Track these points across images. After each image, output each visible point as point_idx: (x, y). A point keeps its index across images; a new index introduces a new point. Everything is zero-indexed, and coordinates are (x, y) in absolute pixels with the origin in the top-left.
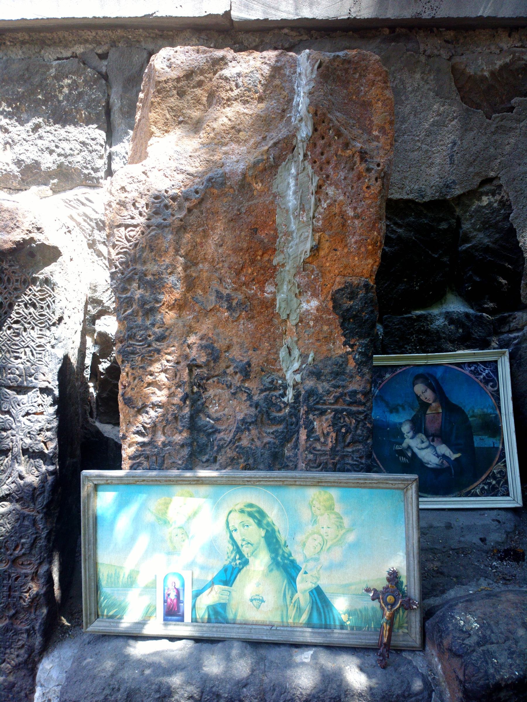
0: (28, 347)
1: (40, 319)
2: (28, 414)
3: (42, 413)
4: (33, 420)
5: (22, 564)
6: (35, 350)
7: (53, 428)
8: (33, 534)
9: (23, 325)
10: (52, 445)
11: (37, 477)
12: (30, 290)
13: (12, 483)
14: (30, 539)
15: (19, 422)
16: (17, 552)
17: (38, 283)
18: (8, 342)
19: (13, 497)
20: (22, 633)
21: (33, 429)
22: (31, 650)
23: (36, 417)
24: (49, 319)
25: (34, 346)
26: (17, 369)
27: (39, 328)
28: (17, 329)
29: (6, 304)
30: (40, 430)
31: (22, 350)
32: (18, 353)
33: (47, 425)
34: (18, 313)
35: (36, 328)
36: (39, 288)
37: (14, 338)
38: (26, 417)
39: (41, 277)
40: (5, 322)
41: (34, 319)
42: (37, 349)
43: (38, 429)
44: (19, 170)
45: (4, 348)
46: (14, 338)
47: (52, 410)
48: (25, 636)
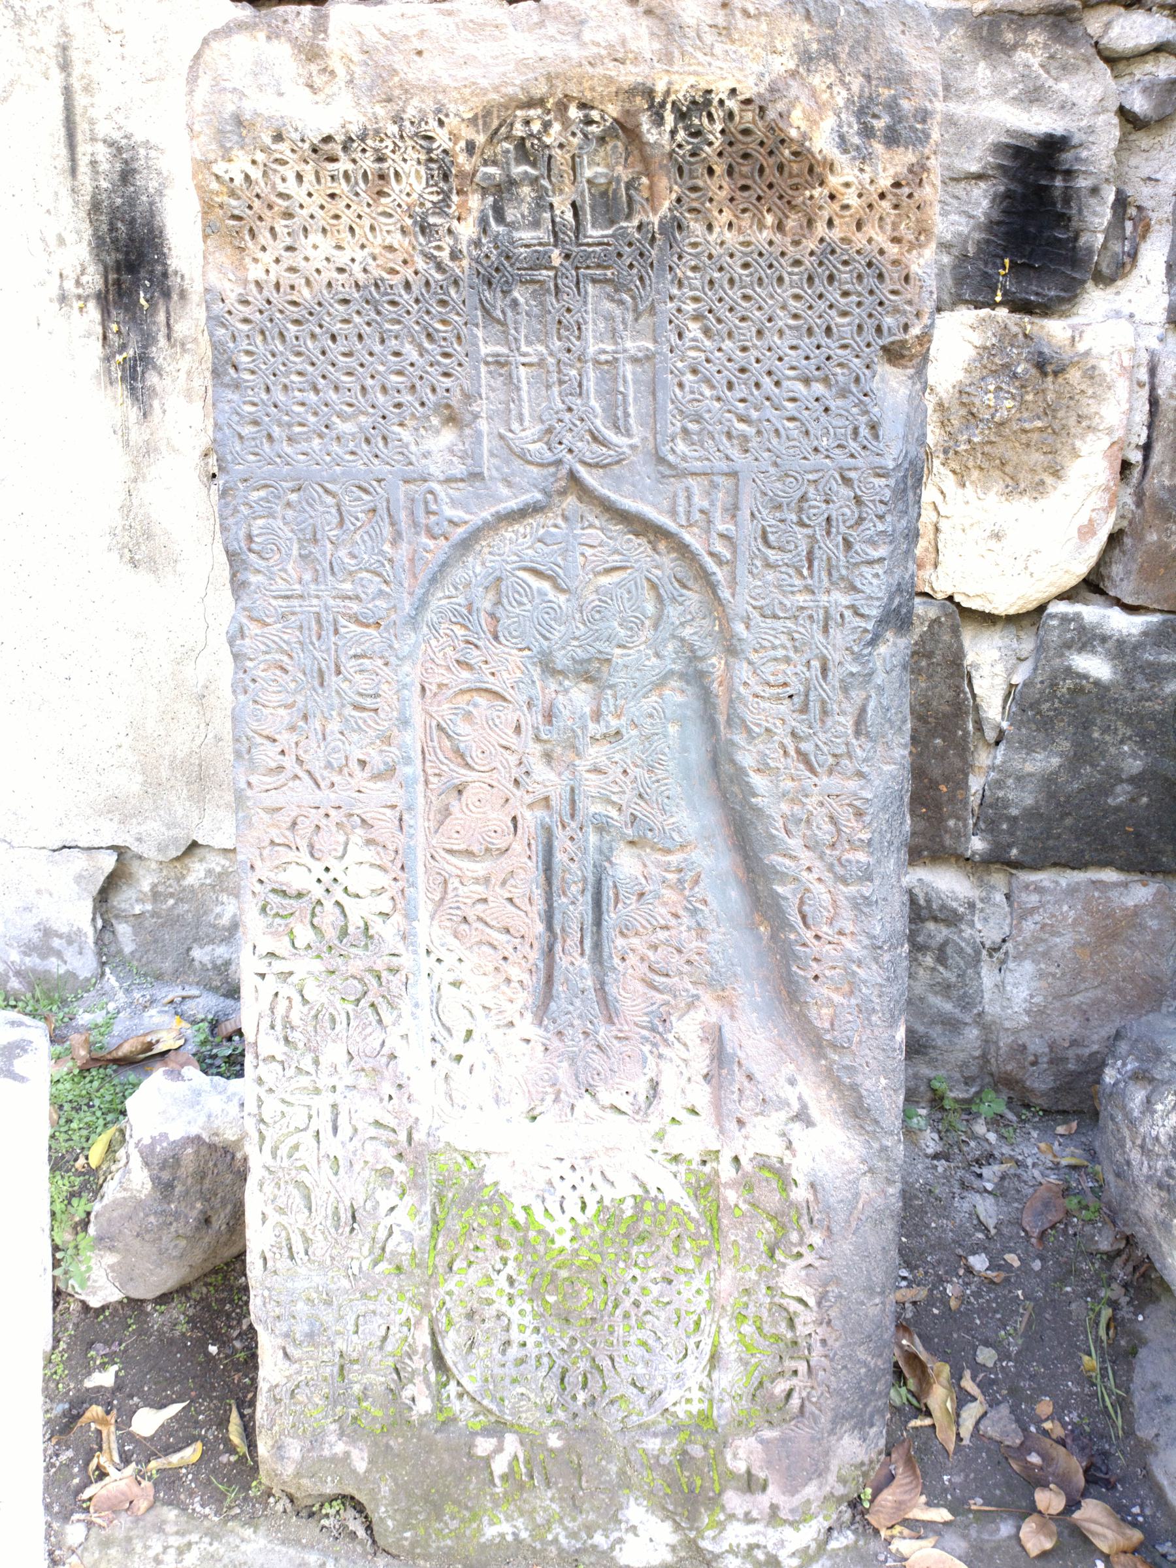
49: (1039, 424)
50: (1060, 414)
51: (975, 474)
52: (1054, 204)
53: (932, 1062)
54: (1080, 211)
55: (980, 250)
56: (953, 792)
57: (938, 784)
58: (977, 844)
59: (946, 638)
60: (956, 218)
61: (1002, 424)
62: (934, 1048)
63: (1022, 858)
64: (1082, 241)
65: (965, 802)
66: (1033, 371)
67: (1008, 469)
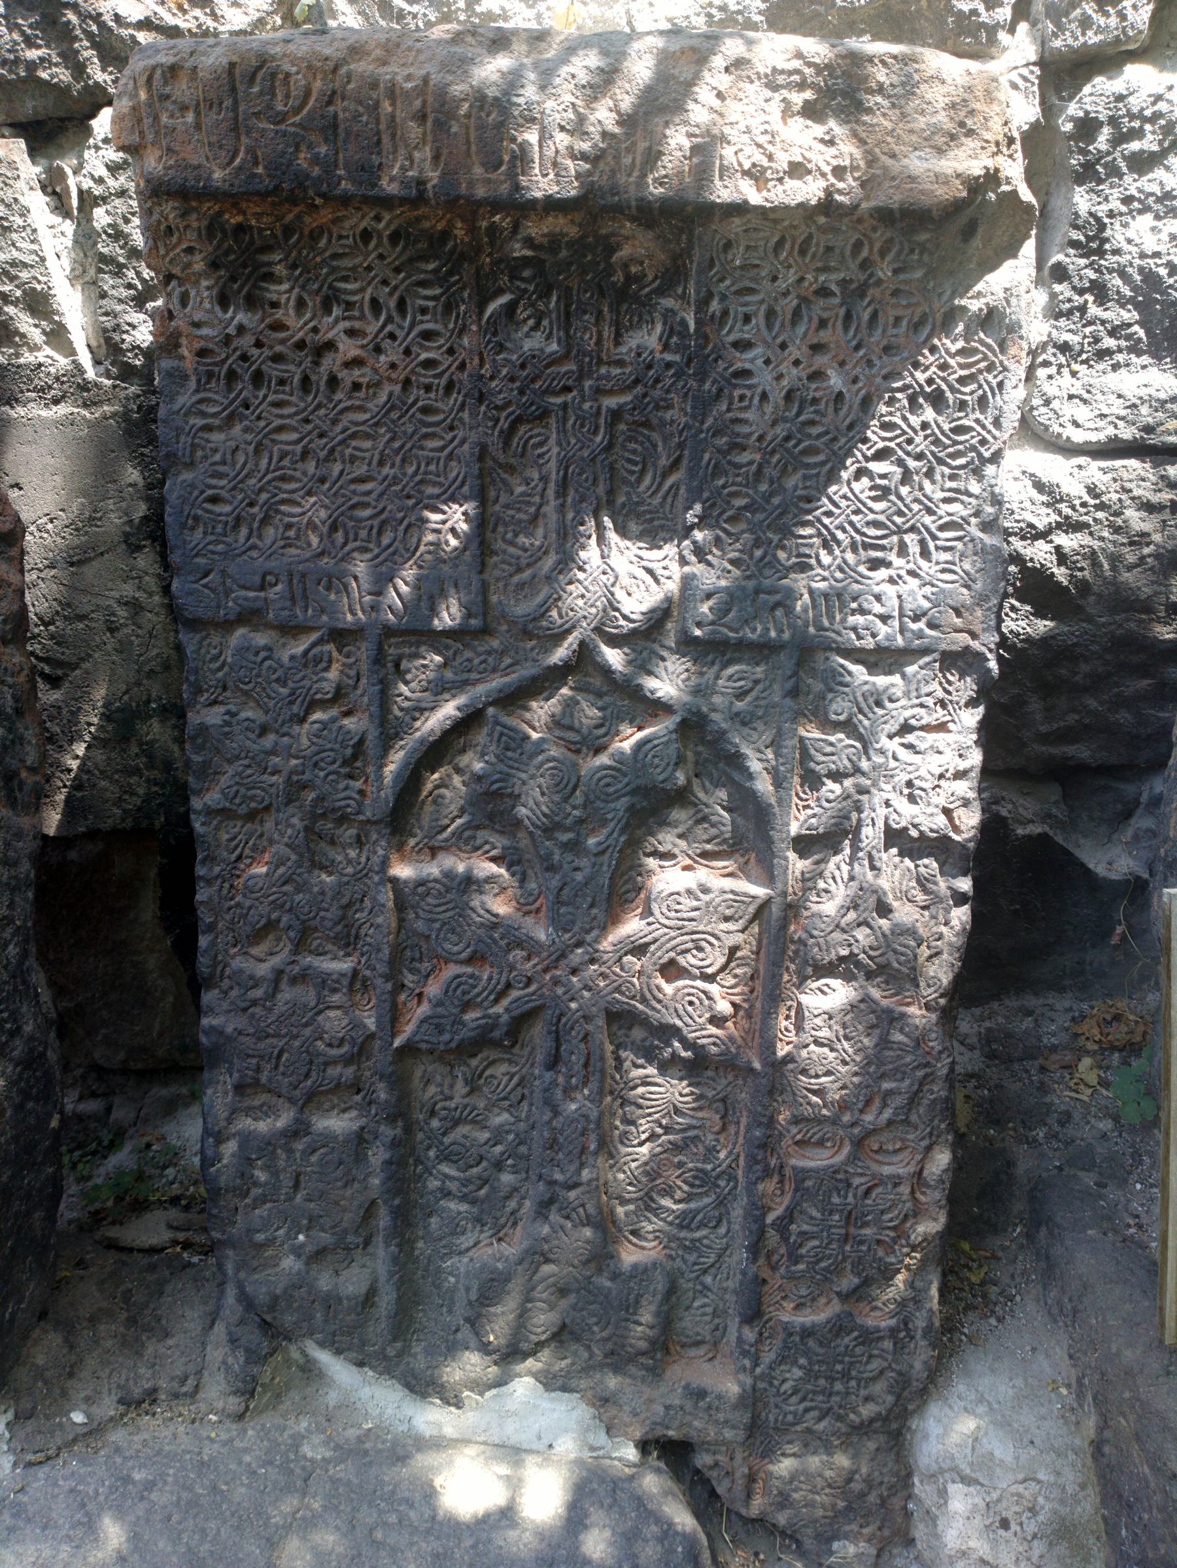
0: (913, 529)
1: (955, 443)
2: (906, 729)
3: (942, 727)
4: (922, 746)
5: (880, 1150)
6: (934, 538)
7: (971, 769)
8: (917, 1067)
9: (900, 463)
10: (970, 819)
11: (924, 908)
12: (933, 349)
13: (859, 925)
14: (907, 1082)
15: (882, 752)
16: (868, 1118)
17: (960, 327)
18: (854, 518)
19: (858, 964)
20: (881, 1338)
21: (923, 772)
22: (902, 1383)
23: (932, 738)
24: (983, 442)
25: (933, 528)
26: (878, 598)
27: (947, 471)
28: (883, 476)
29: (853, 399)
30: (941, 776)
31: (895, 539)
32: (883, 548)
33: (958, 760)
34: (886, 426)
35: (940, 469)
36: (960, 344)
37: (870, 503)
38: (897, 740)
39: (974, 305)
40: (849, 453)
41: (937, 442)
42: (940, 534)
43: (937, 771)
44: (763, 6)
45: (840, 535)
46: (870, 503)
47: (972, 718)
48: (888, 1344)
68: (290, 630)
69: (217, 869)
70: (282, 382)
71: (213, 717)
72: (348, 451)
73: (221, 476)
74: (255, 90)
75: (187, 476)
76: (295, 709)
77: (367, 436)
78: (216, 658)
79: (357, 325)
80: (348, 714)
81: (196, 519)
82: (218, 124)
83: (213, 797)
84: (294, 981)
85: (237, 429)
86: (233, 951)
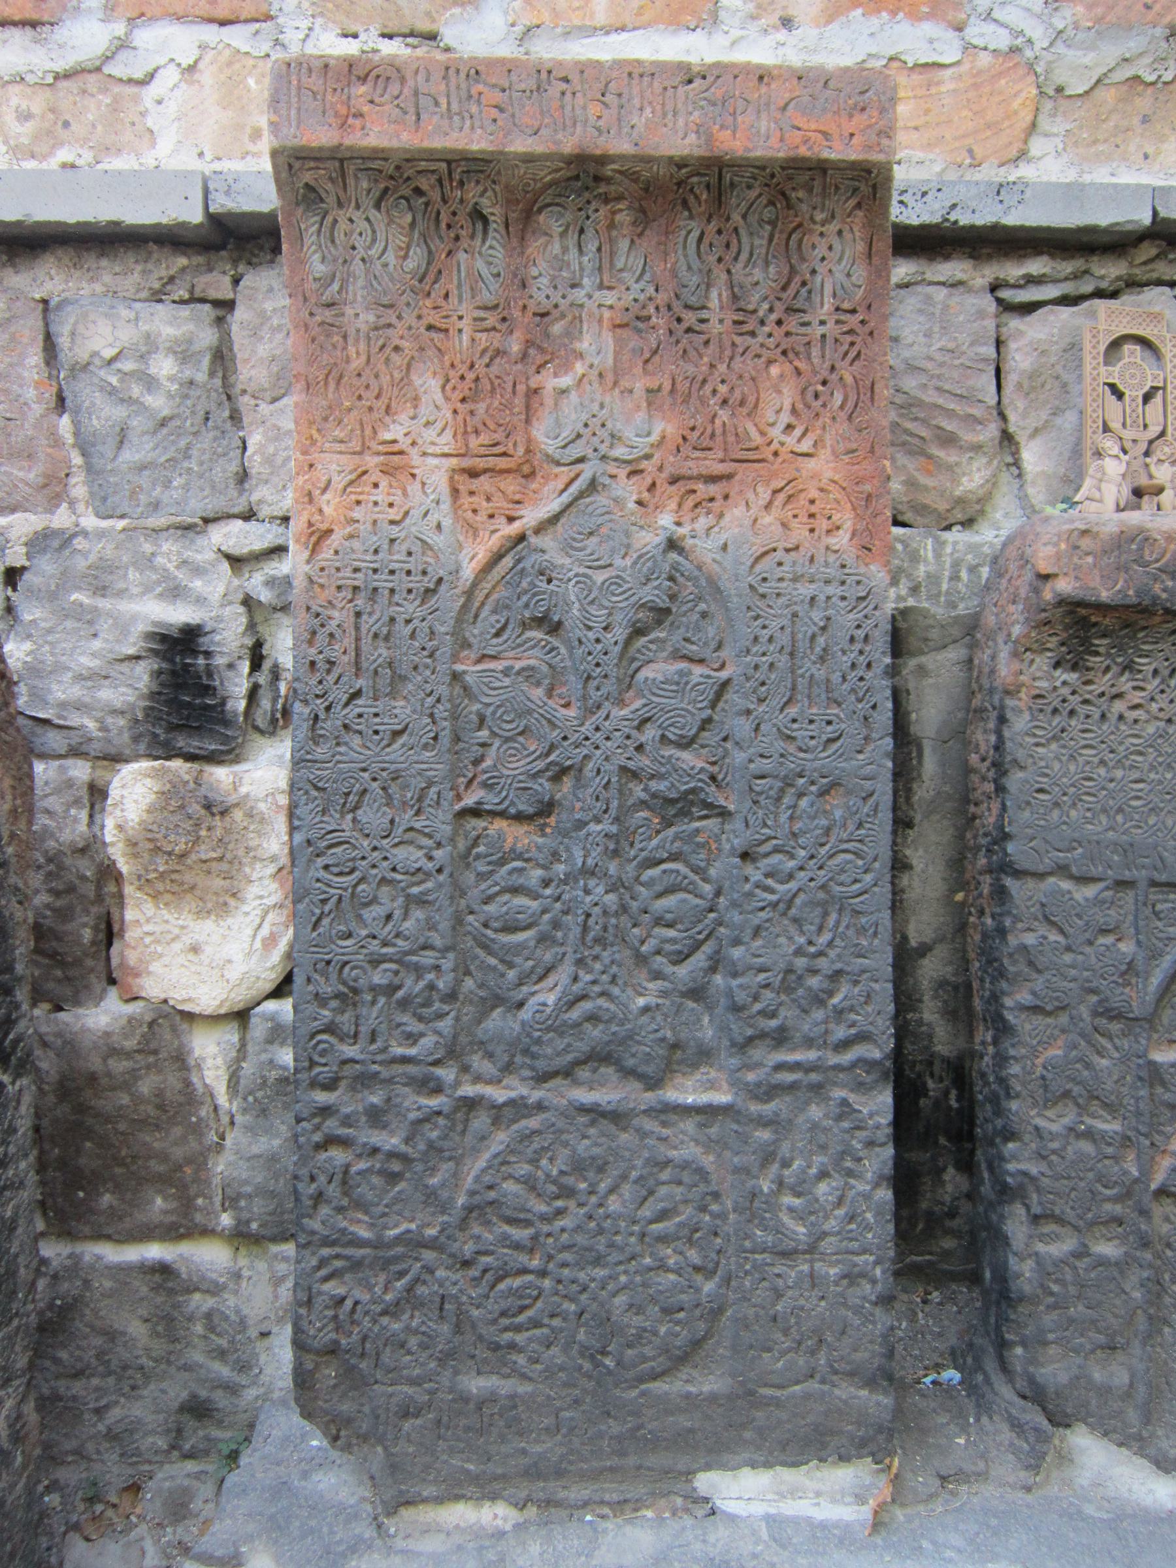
49: (214, 855)
50: (230, 847)
51: (168, 897)
52: (200, 678)
53: (220, 1424)
54: (222, 683)
55: (147, 715)
56: (197, 1171)
57: (181, 1166)
58: (226, 1220)
59: (168, 1036)
60: (123, 689)
61: (183, 855)
62: (217, 1410)
63: (263, 1232)
64: (229, 706)
65: (207, 1181)
66: (203, 812)
67: (198, 892)
68: (1084, 880)
69: (1023, 1051)
70: (1088, 717)
71: (1030, 939)
72: (1127, 763)
73: (1047, 775)
74: (1134, 547)
75: (1020, 775)
76: (1087, 935)
77: (1141, 753)
78: (1030, 898)
79: (1141, 684)
80: (1119, 940)
81: (1028, 803)
82: (1108, 565)
83: (1024, 997)
84: (1080, 1136)
85: (1054, 746)
86: (1032, 1113)
